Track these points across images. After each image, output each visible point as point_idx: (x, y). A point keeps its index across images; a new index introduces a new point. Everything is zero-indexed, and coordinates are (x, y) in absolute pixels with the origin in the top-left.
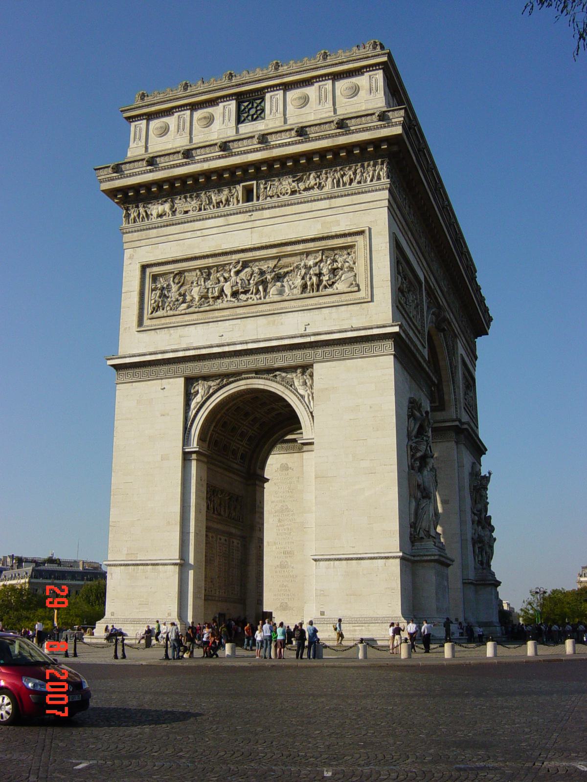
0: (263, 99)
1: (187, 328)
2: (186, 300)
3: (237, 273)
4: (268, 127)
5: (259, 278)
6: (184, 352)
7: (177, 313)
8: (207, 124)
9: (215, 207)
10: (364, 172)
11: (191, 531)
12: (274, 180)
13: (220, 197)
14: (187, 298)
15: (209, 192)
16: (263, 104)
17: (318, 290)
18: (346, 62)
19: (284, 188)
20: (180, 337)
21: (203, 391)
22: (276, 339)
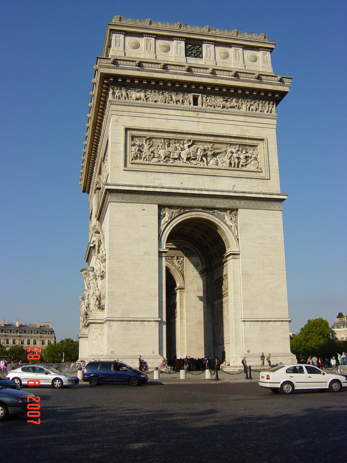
0: (201, 46)
1: (158, 174)
2: (155, 156)
3: (189, 146)
4: (206, 64)
5: (203, 153)
6: (160, 189)
7: (151, 163)
8: (167, 50)
9: (175, 103)
10: (263, 107)
11: (163, 301)
12: (212, 97)
13: (178, 98)
14: (155, 155)
15: (171, 93)
16: (200, 49)
17: (238, 167)
18: (253, 41)
19: (218, 103)
20: (154, 179)
21: (169, 215)
22: (219, 191)
